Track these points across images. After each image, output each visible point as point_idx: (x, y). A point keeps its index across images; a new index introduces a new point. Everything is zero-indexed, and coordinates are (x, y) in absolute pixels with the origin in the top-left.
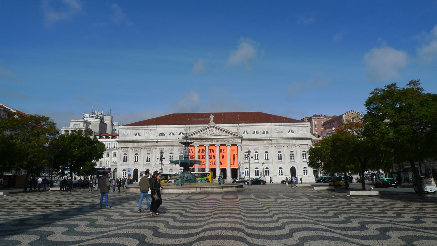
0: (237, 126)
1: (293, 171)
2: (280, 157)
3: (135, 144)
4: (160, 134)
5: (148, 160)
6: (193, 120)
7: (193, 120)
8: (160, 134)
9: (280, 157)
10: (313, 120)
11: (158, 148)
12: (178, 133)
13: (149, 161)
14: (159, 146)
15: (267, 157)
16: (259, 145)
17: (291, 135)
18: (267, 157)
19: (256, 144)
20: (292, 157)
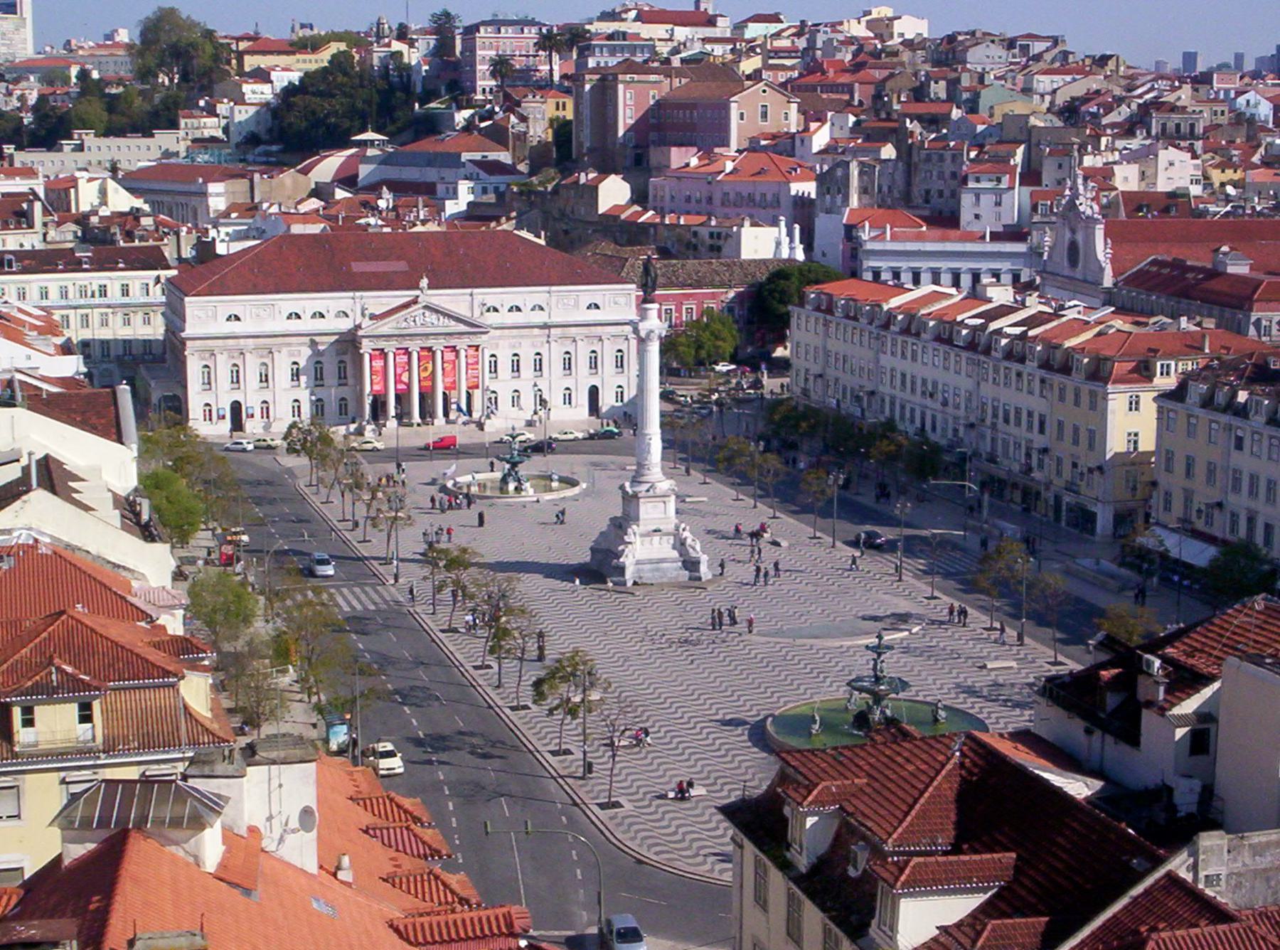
0: (471, 295)
1: (594, 393)
2: (568, 365)
3: (231, 342)
4: (289, 317)
5: (264, 379)
6: (358, 267)
7: (358, 267)
8: (289, 317)
9: (568, 365)
10: (621, 87)
11: (285, 350)
12: (333, 313)
13: (267, 381)
14: (289, 345)
15: (538, 366)
16: (522, 337)
17: (594, 316)
18: (538, 366)
19: (514, 337)
20: (594, 364)
